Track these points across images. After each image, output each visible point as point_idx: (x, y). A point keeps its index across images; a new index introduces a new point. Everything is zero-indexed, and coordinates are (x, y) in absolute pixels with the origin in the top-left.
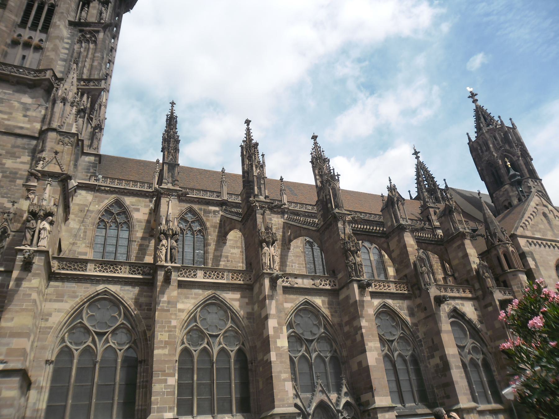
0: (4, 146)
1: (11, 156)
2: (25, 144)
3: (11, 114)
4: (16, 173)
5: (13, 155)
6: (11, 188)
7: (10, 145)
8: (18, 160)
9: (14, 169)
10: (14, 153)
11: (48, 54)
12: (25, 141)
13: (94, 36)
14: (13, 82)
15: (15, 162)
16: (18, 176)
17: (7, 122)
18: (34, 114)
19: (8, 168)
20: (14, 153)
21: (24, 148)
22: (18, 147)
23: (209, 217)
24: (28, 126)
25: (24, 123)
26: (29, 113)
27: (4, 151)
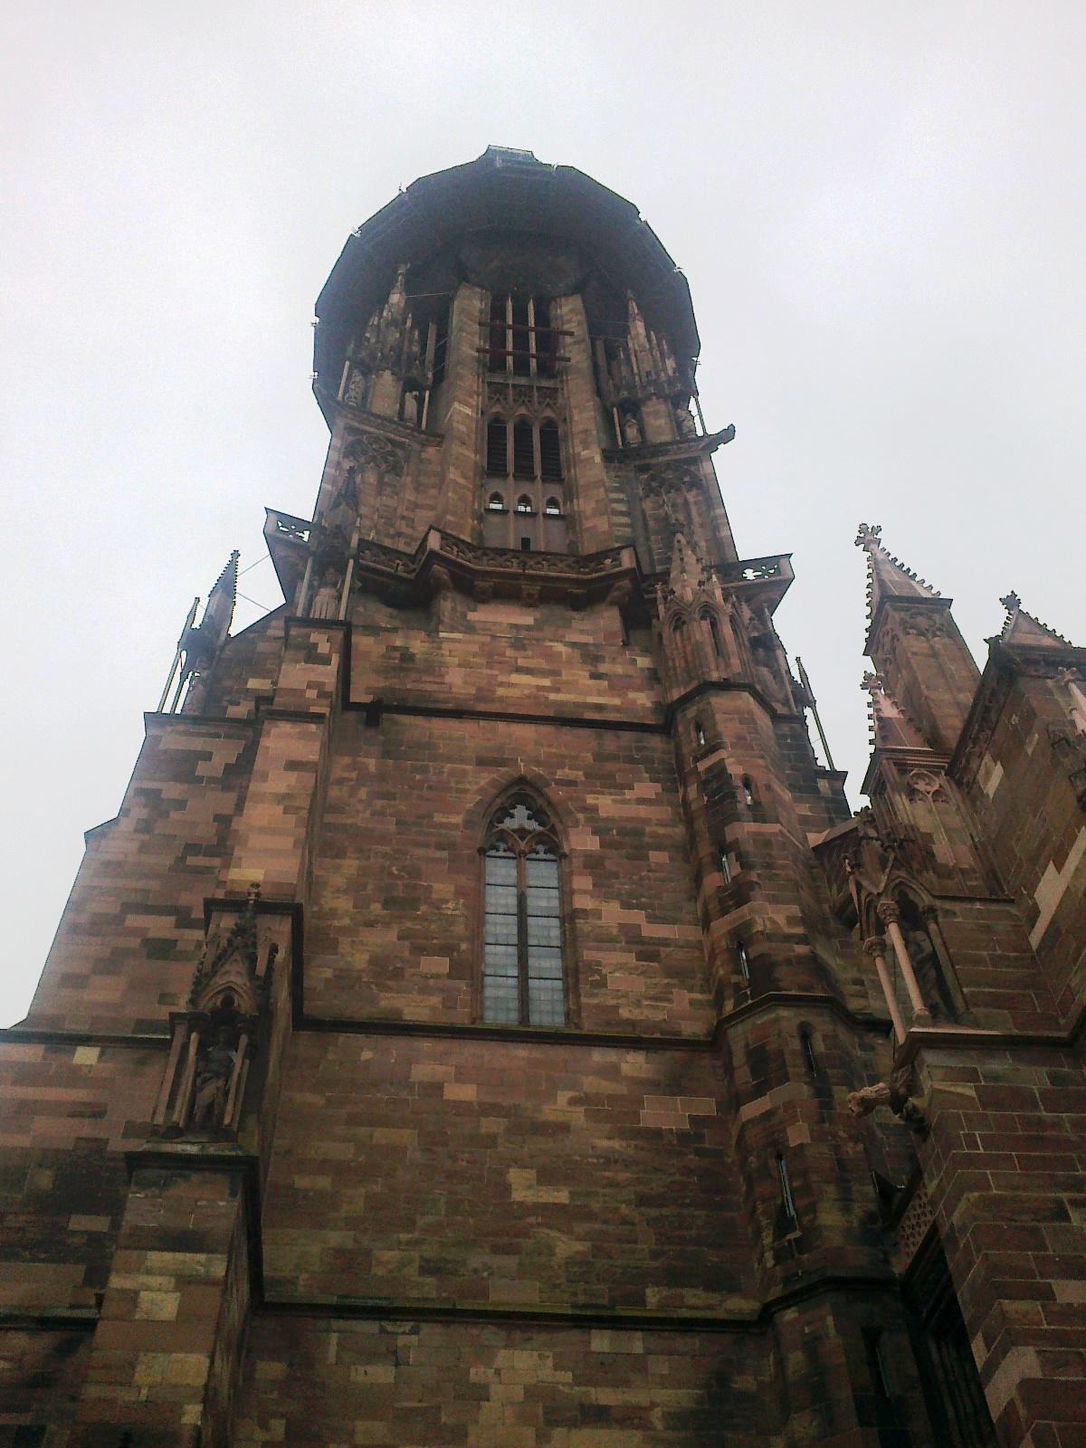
3: (556, 673)
4: (639, 833)
6: (641, 879)
8: (628, 794)
10: (611, 776)
11: (588, 524)
12: (627, 737)
13: (687, 472)
14: (530, 596)
15: (624, 802)
16: (646, 839)
17: (552, 696)
18: (619, 669)
19: (607, 819)
20: (611, 776)
24: (617, 701)
25: (600, 693)
27: (580, 773)
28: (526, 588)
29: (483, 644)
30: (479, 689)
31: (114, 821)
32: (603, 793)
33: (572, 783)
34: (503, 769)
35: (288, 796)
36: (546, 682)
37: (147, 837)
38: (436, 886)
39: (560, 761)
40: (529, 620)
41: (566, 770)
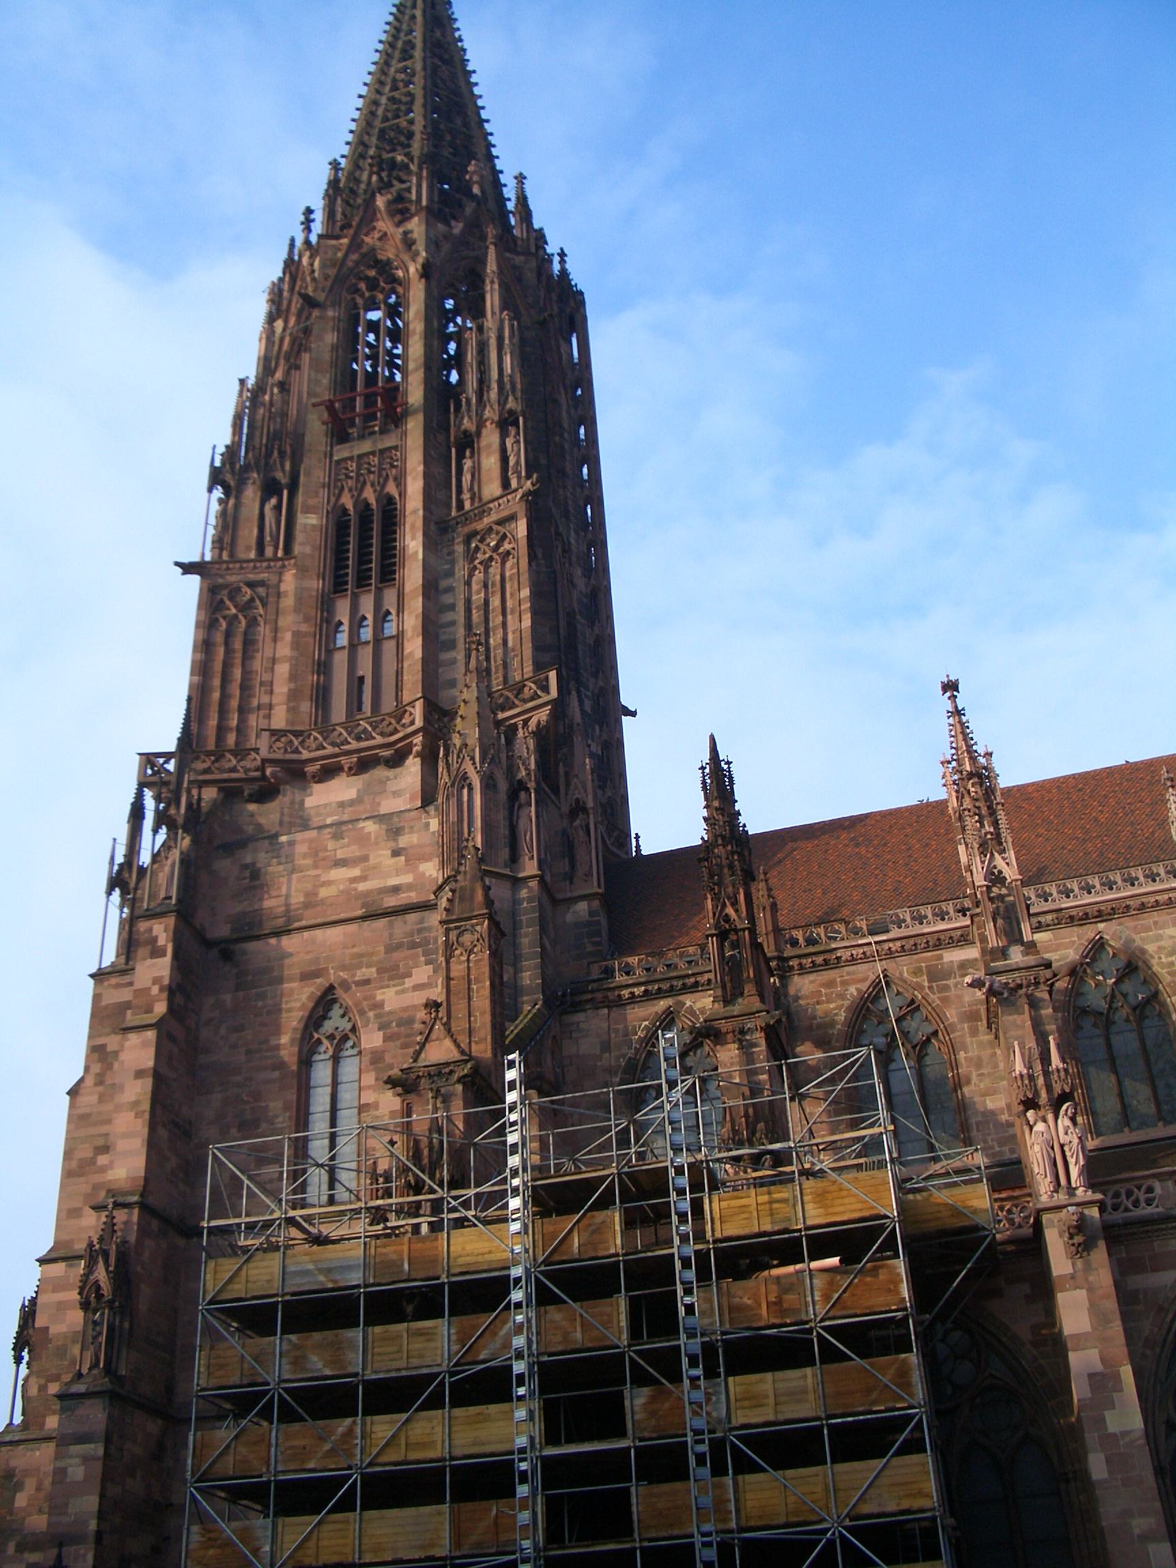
0: (372, 954)
1: (391, 978)
2: (411, 934)
3: (365, 858)
5: (393, 973)
7: (382, 949)
8: (409, 983)
9: (405, 1009)
15: (403, 991)
17: (362, 887)
19: (390, 1013)
21: (413, 945)
22: (399, 946)
23: (946, 988)
24: (407, 879)
26: (403, 841)
28: (345, 761)
29: (311, 841)
30: (307, 895)
31: (82, 1080)
32: (388, 986)
33: (367, 982)
34: (319, 981)
35: (136, 1103)
36: (356, 872)
37: (101, 1088)
38: (272, 1105)
39: (359, 960)
40: (351, 794)
41: (364, 970)
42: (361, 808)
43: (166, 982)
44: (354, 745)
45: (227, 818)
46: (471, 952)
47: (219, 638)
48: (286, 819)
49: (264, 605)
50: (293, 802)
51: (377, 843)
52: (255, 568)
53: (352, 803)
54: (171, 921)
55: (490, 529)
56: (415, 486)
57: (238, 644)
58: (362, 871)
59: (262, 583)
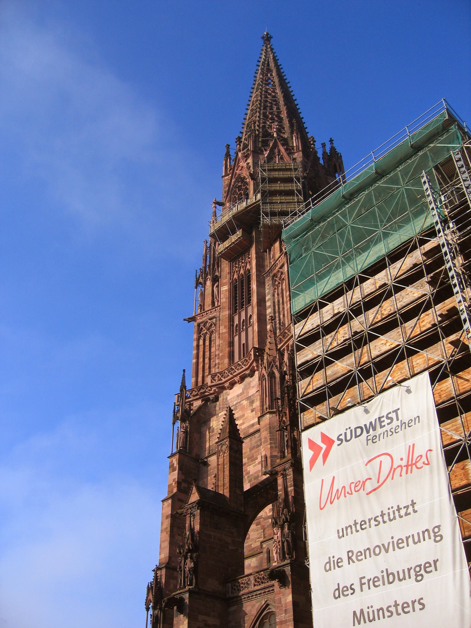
1: (252, 461)
3: (243, 415)
15: (255, 466)
28: (236, 379)
32: (251, 465)
40: (240, 391)
42: (243, 396)
43: (176, 480)
44: (238, 372)
45: (207, 410)
46: (225, 453)
47: (201, 342)
48: (221, 406)
49: (215, 325)
50: (223, 400)
51: (247, 409)
52: (211, 312)
53: (241, 394)
54: (177, 456)
55: (278, 271)
56: (254, 262)
57: (207, 343)
58: (243, 421)
59: (214, 317)
